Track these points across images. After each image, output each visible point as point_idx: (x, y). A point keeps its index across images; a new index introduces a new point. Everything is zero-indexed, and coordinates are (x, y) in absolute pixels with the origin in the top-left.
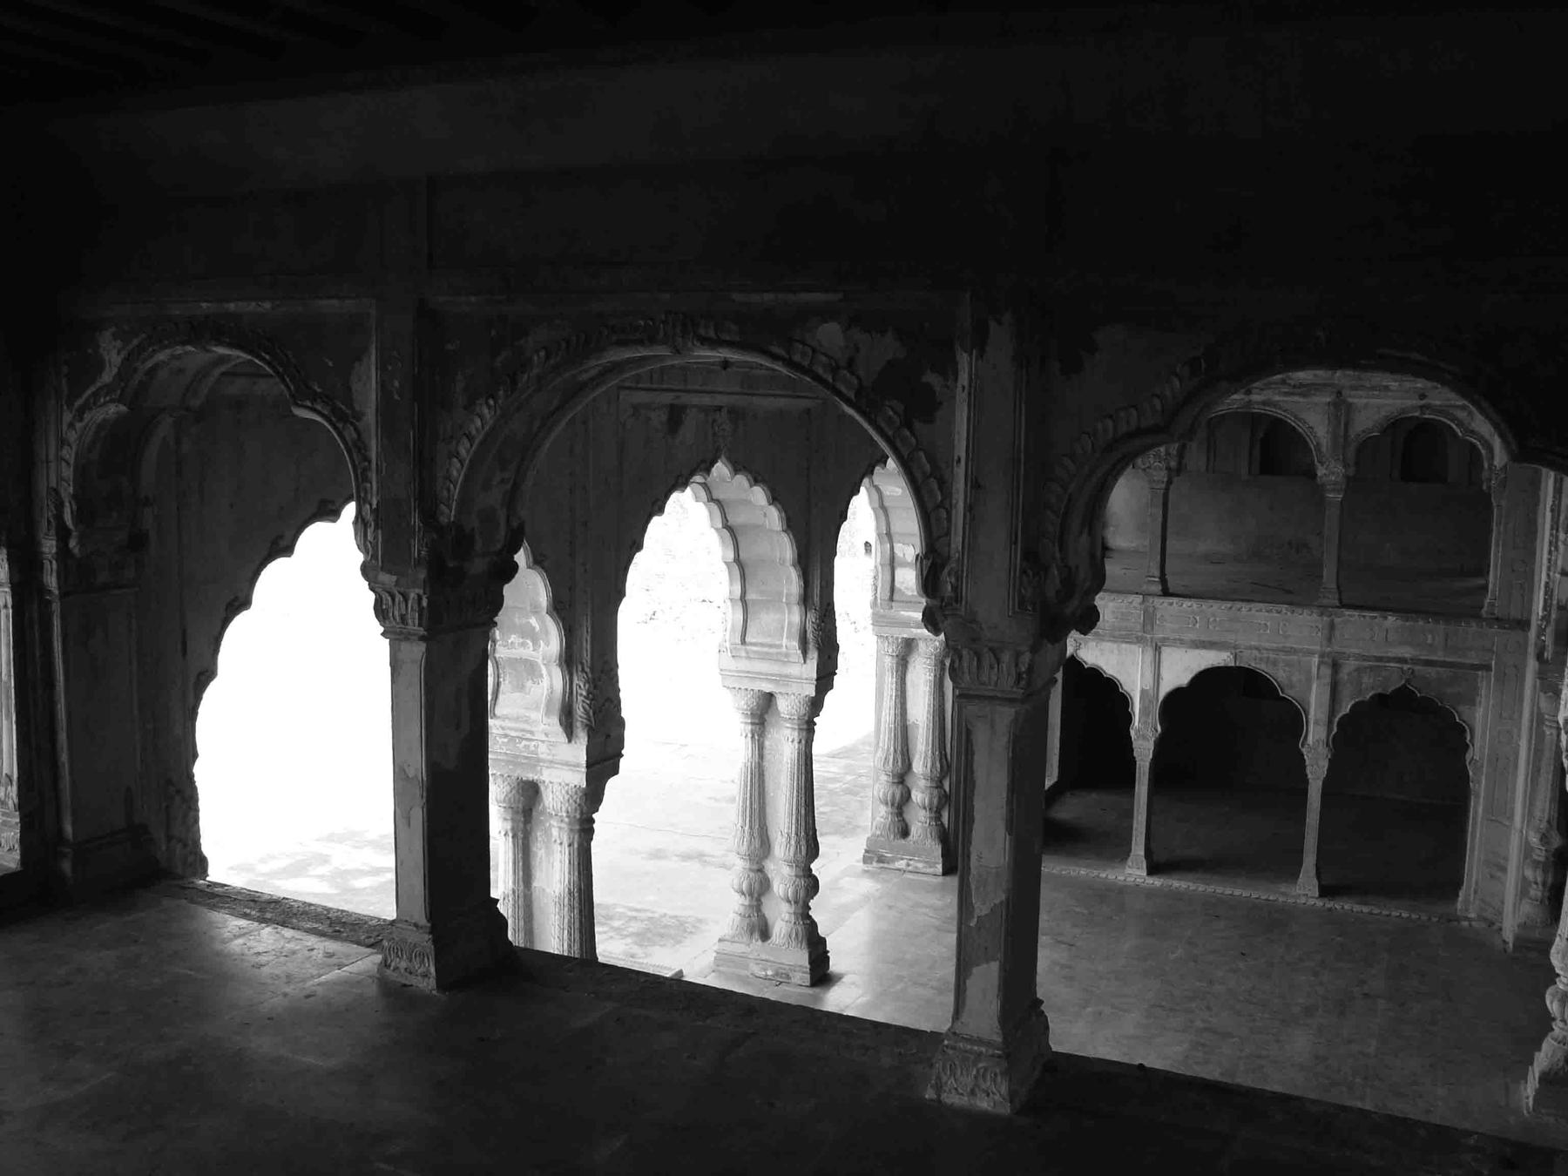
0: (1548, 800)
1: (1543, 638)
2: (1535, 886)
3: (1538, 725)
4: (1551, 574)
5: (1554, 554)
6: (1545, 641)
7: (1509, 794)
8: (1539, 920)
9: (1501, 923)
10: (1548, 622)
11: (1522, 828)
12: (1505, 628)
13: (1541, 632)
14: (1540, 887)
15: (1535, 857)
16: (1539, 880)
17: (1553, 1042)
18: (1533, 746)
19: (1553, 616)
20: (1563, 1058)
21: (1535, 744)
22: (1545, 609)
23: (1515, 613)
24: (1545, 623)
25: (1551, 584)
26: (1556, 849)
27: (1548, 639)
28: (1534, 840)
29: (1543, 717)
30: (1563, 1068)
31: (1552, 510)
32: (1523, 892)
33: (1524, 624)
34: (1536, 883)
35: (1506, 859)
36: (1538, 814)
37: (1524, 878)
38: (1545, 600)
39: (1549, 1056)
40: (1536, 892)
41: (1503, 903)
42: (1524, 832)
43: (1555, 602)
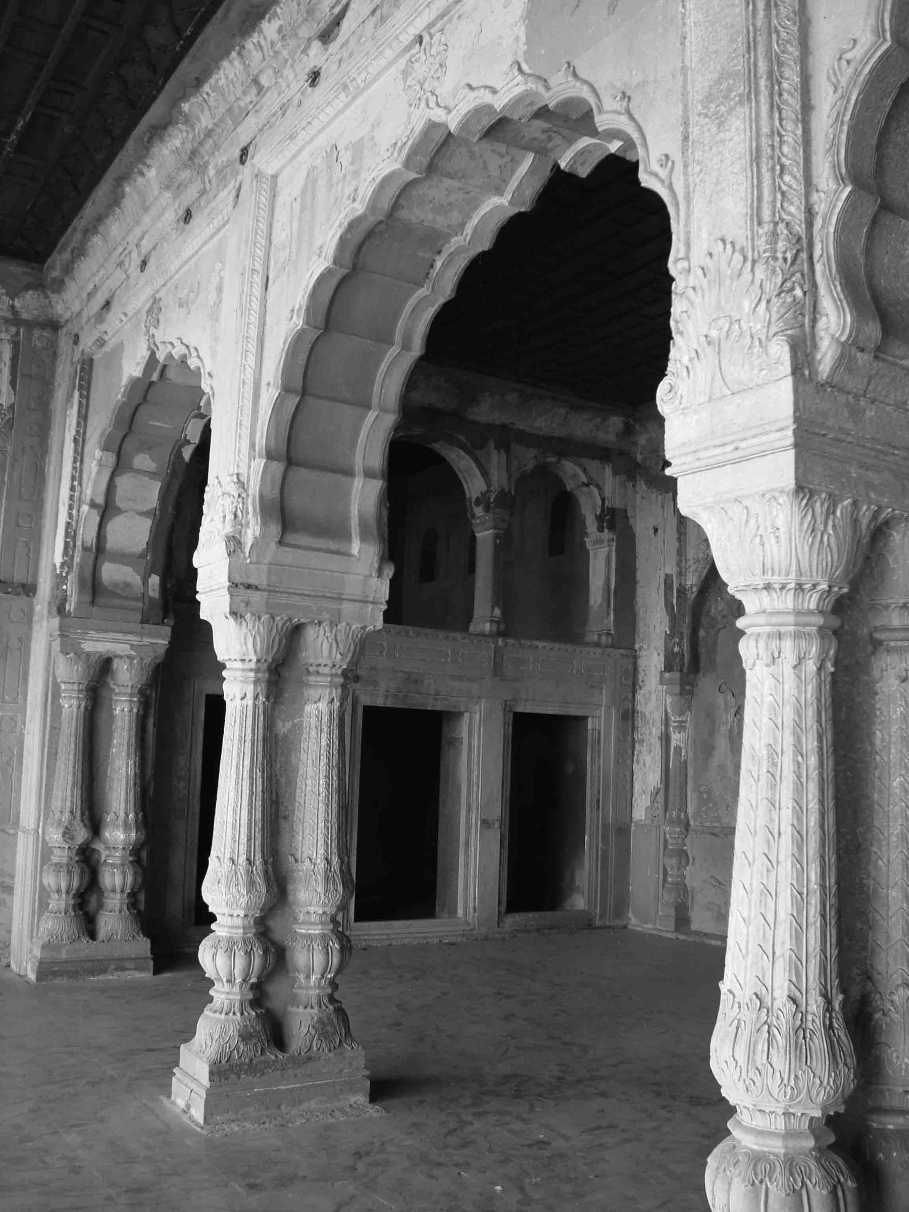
0: (69, 787)
1: (65, 587)
2: (56, 896)
3: (53, 696)
4: (74, 512)
5: (77, 488)
6: (66, 591)
7: (13, 794)
8: (65, 936)
9: (9, 957)
10: (70, 567)
11: (38, 827)
12: (8, 593)
13: (60, 580)
14: (64, 896)
15: (55, 860)
16: (63, 885)
17: (217, 1015)
18: (48, 724)
19: (77, 559)
20: (236, 1034)
21: (51, 721)
22: (65, 552)
23: (19, 576)
24: (66, 570)
25: (74, 523)
26: (80, 846)
27: (71, 587)
28: (55, 836)
29: (60, 687)
30: (237, 1047)
31: (75, 440)
32: (42, 905)
33: (29, 589)
34: (59, 891)
35: (12, 877)
36: (56, 804)
37: (42, 888)
38: (66, 544)
39: (216, 1037)
40: (59, 902)
41: (9, 932)
42: (40, 831)
43: (79, 543)
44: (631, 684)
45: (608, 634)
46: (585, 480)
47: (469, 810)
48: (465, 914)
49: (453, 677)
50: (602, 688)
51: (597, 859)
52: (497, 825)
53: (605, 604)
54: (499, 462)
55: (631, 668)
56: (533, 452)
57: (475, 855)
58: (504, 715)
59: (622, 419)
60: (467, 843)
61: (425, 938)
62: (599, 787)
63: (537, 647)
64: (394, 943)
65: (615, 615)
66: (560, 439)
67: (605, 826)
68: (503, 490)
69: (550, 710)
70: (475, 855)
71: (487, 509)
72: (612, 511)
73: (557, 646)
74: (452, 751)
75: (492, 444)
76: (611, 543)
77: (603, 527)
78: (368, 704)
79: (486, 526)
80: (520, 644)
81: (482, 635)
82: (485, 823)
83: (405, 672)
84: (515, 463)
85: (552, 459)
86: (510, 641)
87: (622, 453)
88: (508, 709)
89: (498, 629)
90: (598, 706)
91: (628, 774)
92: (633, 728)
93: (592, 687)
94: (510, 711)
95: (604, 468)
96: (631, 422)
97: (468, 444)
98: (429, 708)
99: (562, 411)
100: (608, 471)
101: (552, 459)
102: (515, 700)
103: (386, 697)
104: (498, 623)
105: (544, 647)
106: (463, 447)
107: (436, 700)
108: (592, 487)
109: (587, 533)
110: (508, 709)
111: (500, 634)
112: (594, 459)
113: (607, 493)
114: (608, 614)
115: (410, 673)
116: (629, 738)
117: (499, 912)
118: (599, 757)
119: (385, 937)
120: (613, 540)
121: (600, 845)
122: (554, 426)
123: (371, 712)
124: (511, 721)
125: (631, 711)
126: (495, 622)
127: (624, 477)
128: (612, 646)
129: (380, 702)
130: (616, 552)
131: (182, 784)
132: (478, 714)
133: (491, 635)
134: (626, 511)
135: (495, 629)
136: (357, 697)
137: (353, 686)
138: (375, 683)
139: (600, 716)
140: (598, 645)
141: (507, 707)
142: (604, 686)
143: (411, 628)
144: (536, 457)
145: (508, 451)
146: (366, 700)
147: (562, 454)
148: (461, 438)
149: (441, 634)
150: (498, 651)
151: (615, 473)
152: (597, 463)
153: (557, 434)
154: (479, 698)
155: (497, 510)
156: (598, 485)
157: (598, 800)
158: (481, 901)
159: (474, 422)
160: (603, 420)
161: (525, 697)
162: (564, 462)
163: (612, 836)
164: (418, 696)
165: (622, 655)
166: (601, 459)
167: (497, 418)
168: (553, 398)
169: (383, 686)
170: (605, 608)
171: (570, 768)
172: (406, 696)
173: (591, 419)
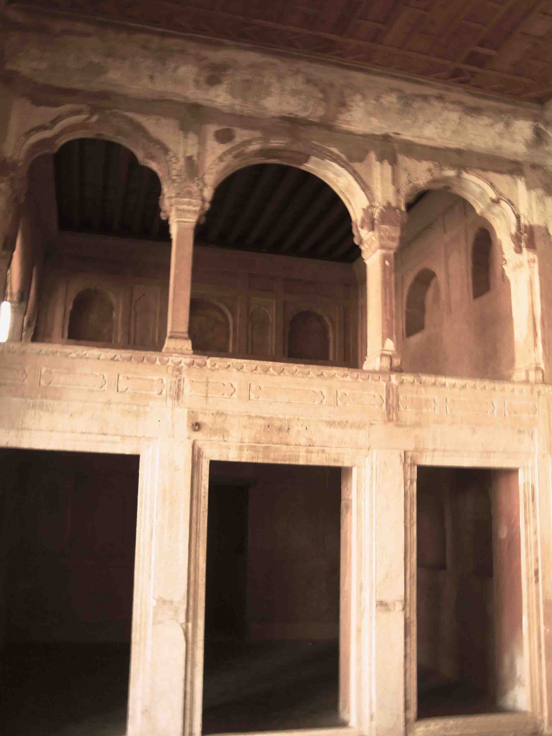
46: (494, 196)
47: (361, 588)
48: (360, 722)
49: (331, 424)
52: (399, 606)
53: (532, 334)
54: (382, 175)
56: (425, 165)
57: (370, 647)
59: (531, 123)
60: (359, 631)
62: (536, 553)
63: (444, 385)
65: (544, 348)
66: (459, 152)
68: (389, 204)
70: (370, 647)
71: (372, 228)
72: (531, 230)
73: (470, 383)
74: (349, 514)
75: (373, 156)
76: (532, 265)
77: (520, 247)
78: (216, 458)
79: (373, 247)
81: (374, 372)
82: (382, 605)
83: (264, 418)
84: (403, 178)
85: (450, 173)
86: (408, 378)
87: (534, 167)
88: (409, 461)
89: (391, 364)
93: (519, 432)
94: (412, 465)
95: (516, 183)
96: (542, 127)
97: (343, 156)
99: (455, 116)
100: (521, 185)
101: (450, 173)
102: (416, 450)
103: (241, 449)
104: (391, 357)
105: (454, 386)
106: (336, 159)
108: (503, 204)
109: (504, 260)
110: (409, 461)
111: (393, 370)
112: (501, 172)
113: (523, 210)
114: (536, 345)
115: (271, 418)
117: (407, 721)
118: (535, 516)
120: (534, 261)
121: (542, 627)
122: (448, 134)
124: (415, 477)
126: (386, 355)
127: (540, 192)
128: (544, 382)
129: (233, 456)
130: (540, 274)
132: (368, 469)
133: (381, 372)
134: (547, 229)
135: (386, 363)
136: (199, 450)
137: (198, 436)
138: (223, 432)
139: (533, 469)
140: (527, 382)
142: (536, 430)
143: (270, 363)
144: (430, 170)
145: (394, 162)
147: (462, 167)
148: (335, 150)
151: (529, 187)
152: (506, 178)
153: (453, 145)
155: (384, 226)
156: (509, 201)
157: (536, 573)
160: (508, 125)
161: (431, 447)
162: (465, 175)
164: (284, 447)
168: (440, 98)
169: (235, 436)
170: (531, 339)
171: (503, 533)
172: (267, 448)
173: (492, 125)
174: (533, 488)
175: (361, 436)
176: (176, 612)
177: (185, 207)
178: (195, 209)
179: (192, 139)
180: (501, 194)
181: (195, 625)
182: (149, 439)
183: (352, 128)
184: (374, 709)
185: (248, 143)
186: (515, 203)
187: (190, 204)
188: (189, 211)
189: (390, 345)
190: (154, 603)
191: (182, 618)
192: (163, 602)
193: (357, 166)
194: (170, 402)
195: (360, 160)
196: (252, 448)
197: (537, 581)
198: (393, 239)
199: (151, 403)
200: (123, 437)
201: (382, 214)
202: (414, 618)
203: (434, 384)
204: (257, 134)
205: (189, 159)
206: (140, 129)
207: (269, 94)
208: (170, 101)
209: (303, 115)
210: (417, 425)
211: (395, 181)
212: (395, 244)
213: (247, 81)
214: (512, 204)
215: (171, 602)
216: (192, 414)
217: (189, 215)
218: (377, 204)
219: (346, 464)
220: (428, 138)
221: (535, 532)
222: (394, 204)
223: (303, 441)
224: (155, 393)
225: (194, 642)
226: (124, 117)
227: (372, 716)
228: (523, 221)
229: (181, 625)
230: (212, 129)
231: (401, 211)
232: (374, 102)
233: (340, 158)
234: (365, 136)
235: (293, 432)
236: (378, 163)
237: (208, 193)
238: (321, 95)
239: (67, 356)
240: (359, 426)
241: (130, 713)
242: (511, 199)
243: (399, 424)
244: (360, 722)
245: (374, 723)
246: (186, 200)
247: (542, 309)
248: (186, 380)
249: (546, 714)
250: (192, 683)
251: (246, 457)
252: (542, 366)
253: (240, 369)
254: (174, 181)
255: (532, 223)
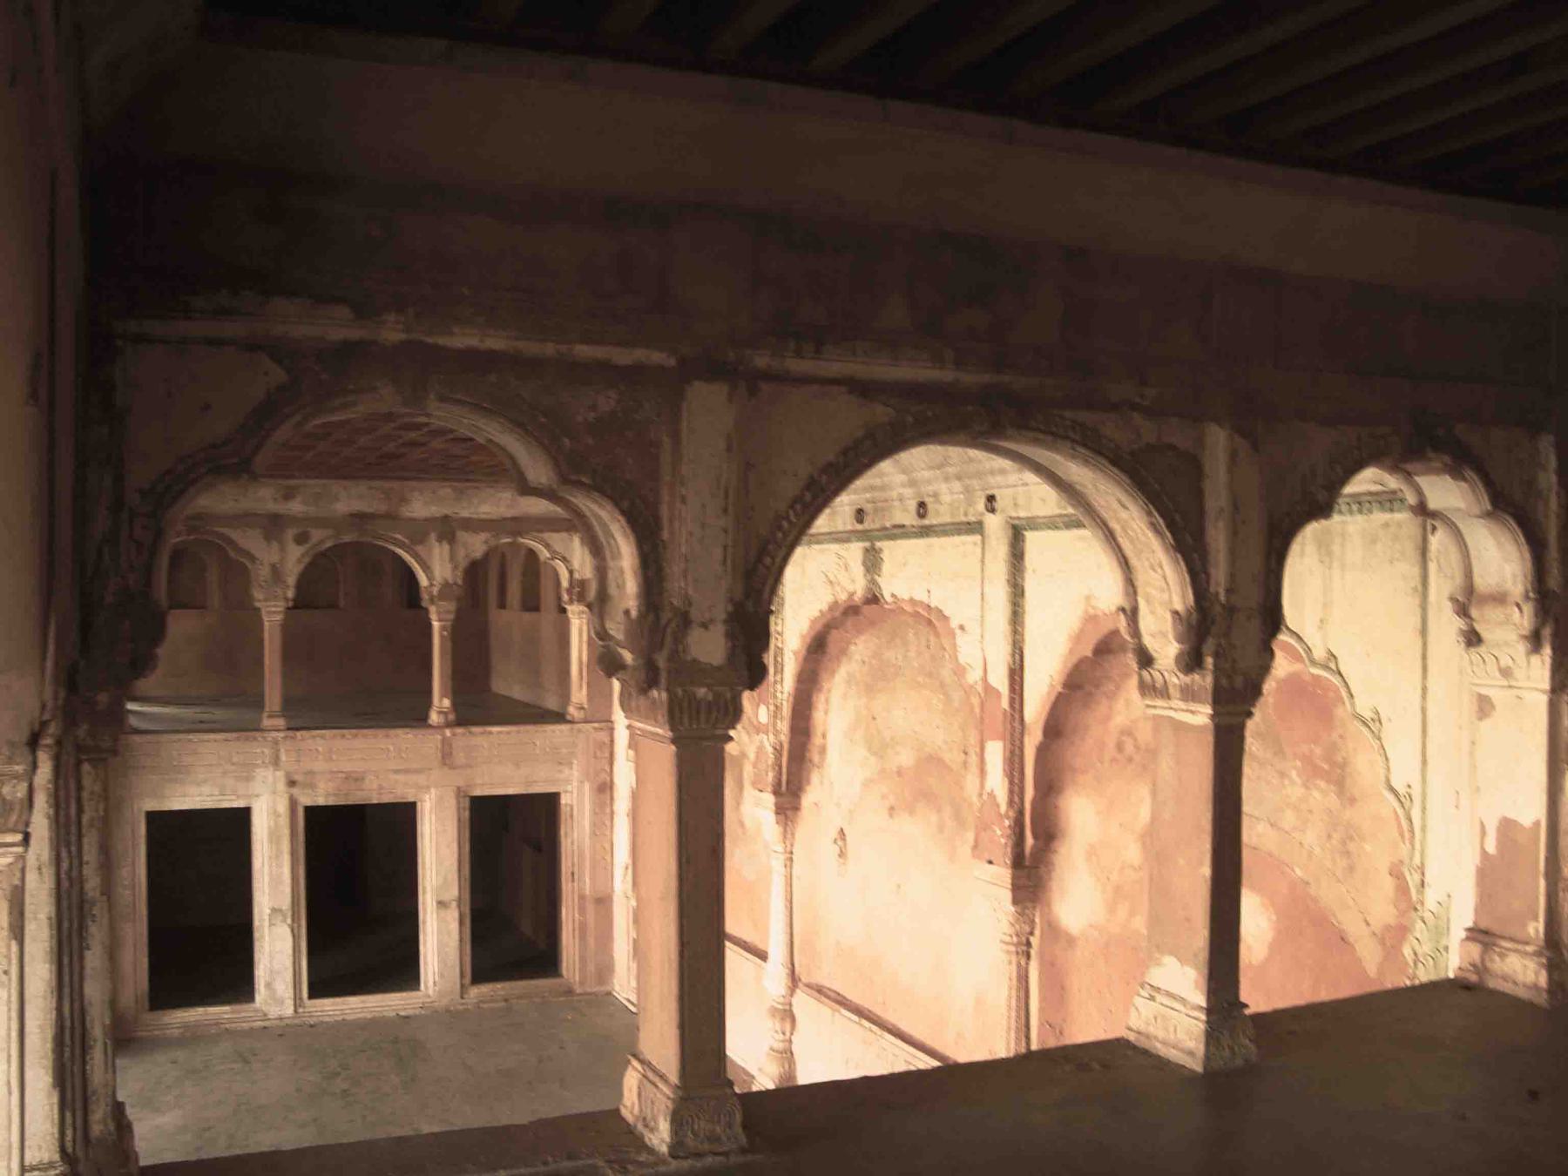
44: (607, 755)
45: (582, 708)
49: (397, 772)
50: (572, 763)
51: (574, 930)
52: (454, 904)
55: (607, 740)
56: (483, 536)
58: (458, 803)
61: (381, 1012)
64: (348, 1017)
66: (514, 519)
67: (582, 897)
69: (511, 791)
75: (433, 536)
78: (309, 804)
80: (470, 732)
82: (441, 904)
84: (461, 553)
86: (459, 730)
90: (568, 781)
91: (607, 846)
92: (612, 799)
94: (465, 797)
95: (571, 540)
98: (375, 802)
107: (380, 794)
110: (462, 794)
111: (448, 725)
113: (576, 564)
114: (581, 686)
116: (608, 810)
117: (462, 986)
119: (359, 1010)
121: (577, 915)
123: (311, 811)
125: (609, 784)
128: (586, 721)
129: (321, 801)
131: (128, 892)
137: (295, 791)
138: (312, 786)
139: (572, 792)
141: (459, 792)
142: (575, 762)
144: (486, 542)
146: (306, 800)
147: (520, 534)
148: (399, 536)
149: (381, 733)
150: (444, 740)
154: (428, 787)
157: (573, 874)
158: (442, 975)
159: (414, 520)
163: (590, 908)
165: (595, 729)
166: (568, 530)
167: (435, 511)
169: (320, 791)
174: (572, 809)
175: (421, 779)
176: (285, 916)
177: (273, 609)
178: (279, 609)
179: (275, 545)
180: (558, 553)
181: (299, 926)
182: (257, 796)
183: (415, 515)
184: (437, 979)
185: (322, 542)
186: (568, 558)
187: (275, 606)
188: (274, 612)
189: (447, 703)
190: (268, 911)
191: (289, 921)
192: (274, 910)
193: (419, 548)
194: (271, 769)
195: (421, 542)
196: (335, 795)
197: (573, 881)
198: (448, 612)
199: (257, 770)
200: (238, 797)
201: (440, 591)
202: (467, 911)
203: (482, 733)
204: (330, 532)
205: (273, 566)
206: (231, 542)
207: (337, 500)
208: (256, 515)
209: (370, 510)
210: (470, 766)
211: (452, 558)
212: (452, 616)
213: (320, 493)
214: (568, 561)
215: (280, 910)
216: (288, 775)
217: (275, 615)
218: (435, 583)
219: (411, 799)
220: (484, 513)
221: (572, 843)
222: (451, 581)
223: (375, 786)
224: (259, 762)
225: (299, 937)
226: (216, 532)
227: (434, 982)
228: (577, 576)
229: (289, 925)
230: (290, 533)
231: (458, 586)
232: (431, 495)
233: (404, 543)
234: (426, 520)
235: (367, 781)
236: (437, 544)
237: (290, 594)
238: (382, 496)
239: (190, 740)
240: (417, 771)
241: (256, 986)
242: (566, 555)
243: (452, 767)
244: (426, 987)
245: (437, 988)
246: (273, 603)
247: (589, 655)
248: (282, 750)
249: (577, 979)
250: (300, 965)
251: (331, 802)
252: (586, 706)
253: (323, 737)
254: (260, 585)
255: (585, 577)
